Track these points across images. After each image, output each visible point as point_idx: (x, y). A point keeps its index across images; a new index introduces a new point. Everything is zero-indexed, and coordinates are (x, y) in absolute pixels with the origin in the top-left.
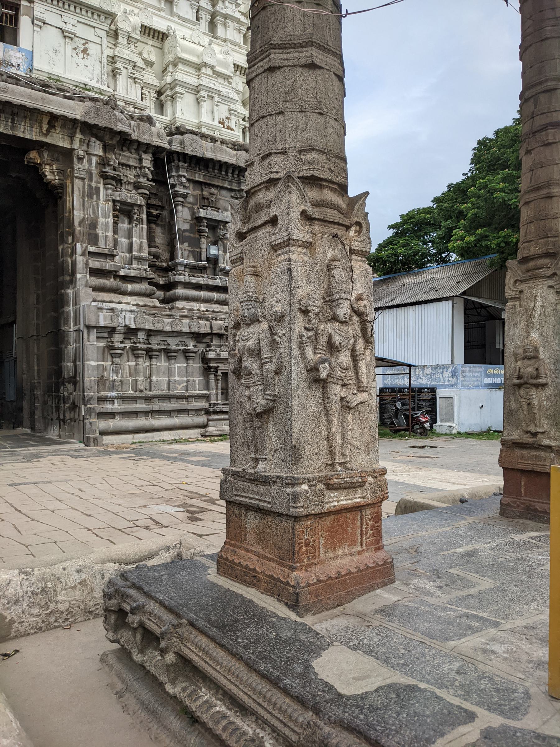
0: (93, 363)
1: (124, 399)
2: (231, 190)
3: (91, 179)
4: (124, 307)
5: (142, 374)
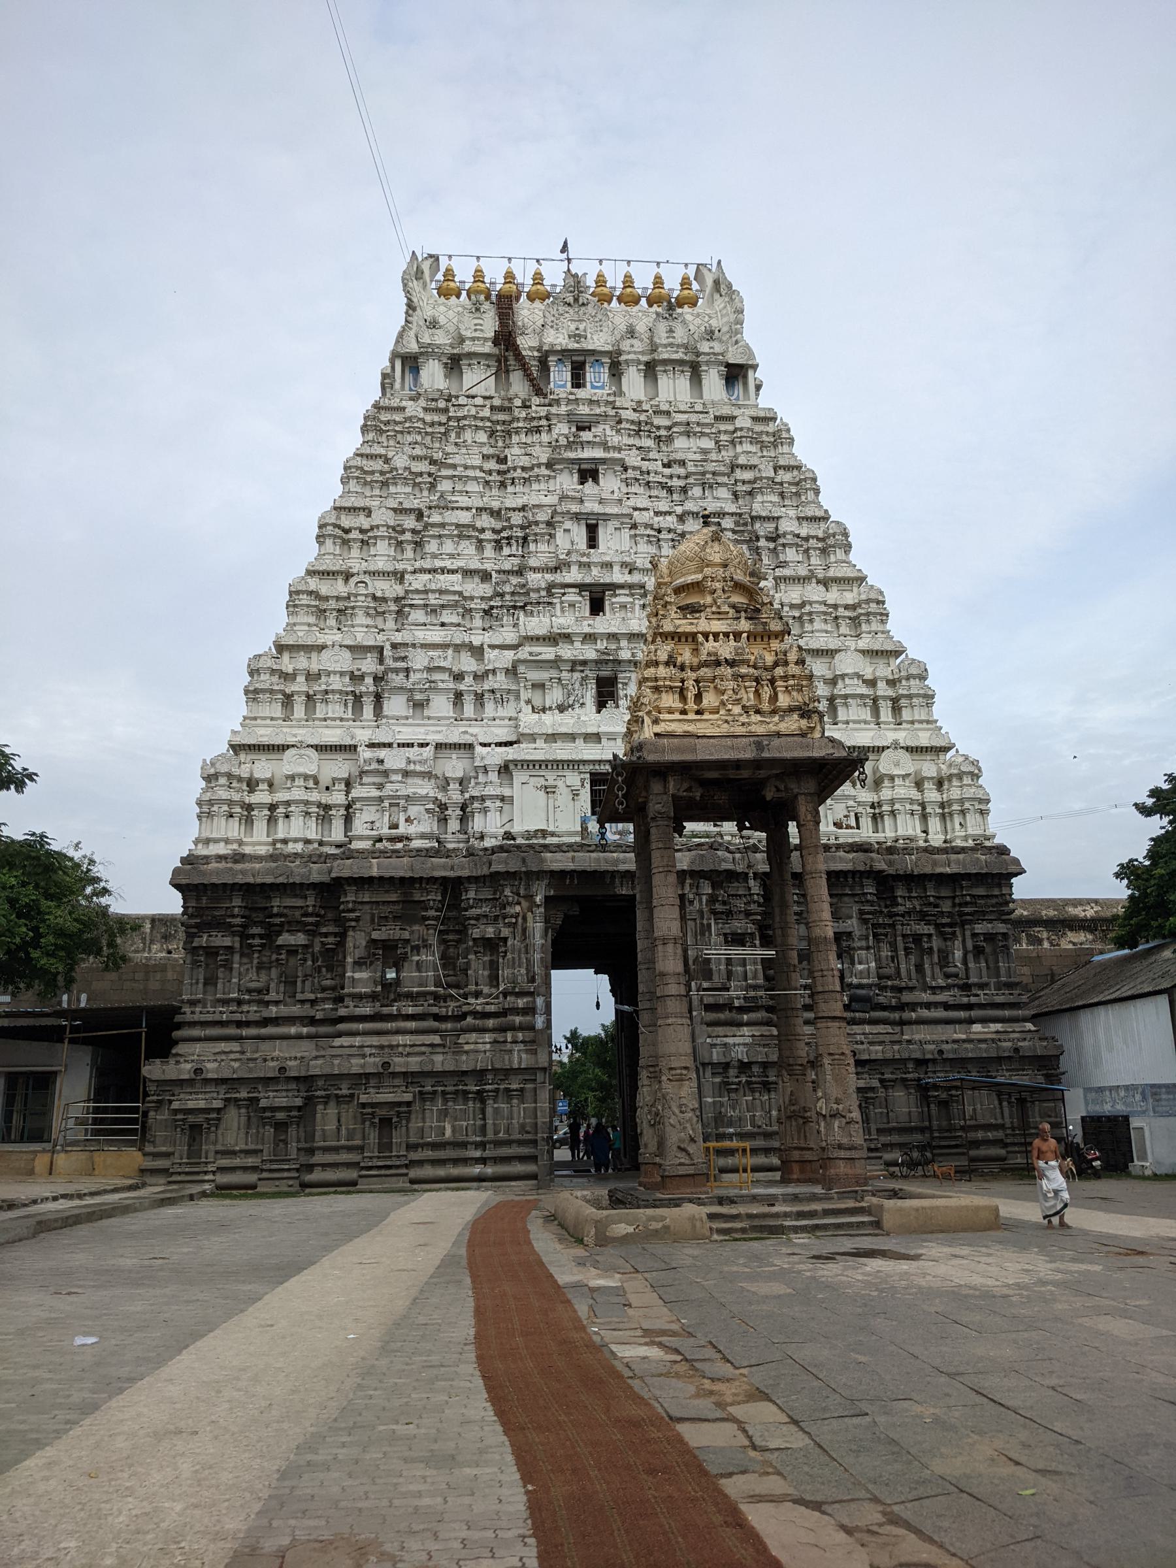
0: (710, 1100)
1: (742, 1136)
2: (854, 895)
3: (702, 918)
4: (737, 1040)
5: (759, 1109)
